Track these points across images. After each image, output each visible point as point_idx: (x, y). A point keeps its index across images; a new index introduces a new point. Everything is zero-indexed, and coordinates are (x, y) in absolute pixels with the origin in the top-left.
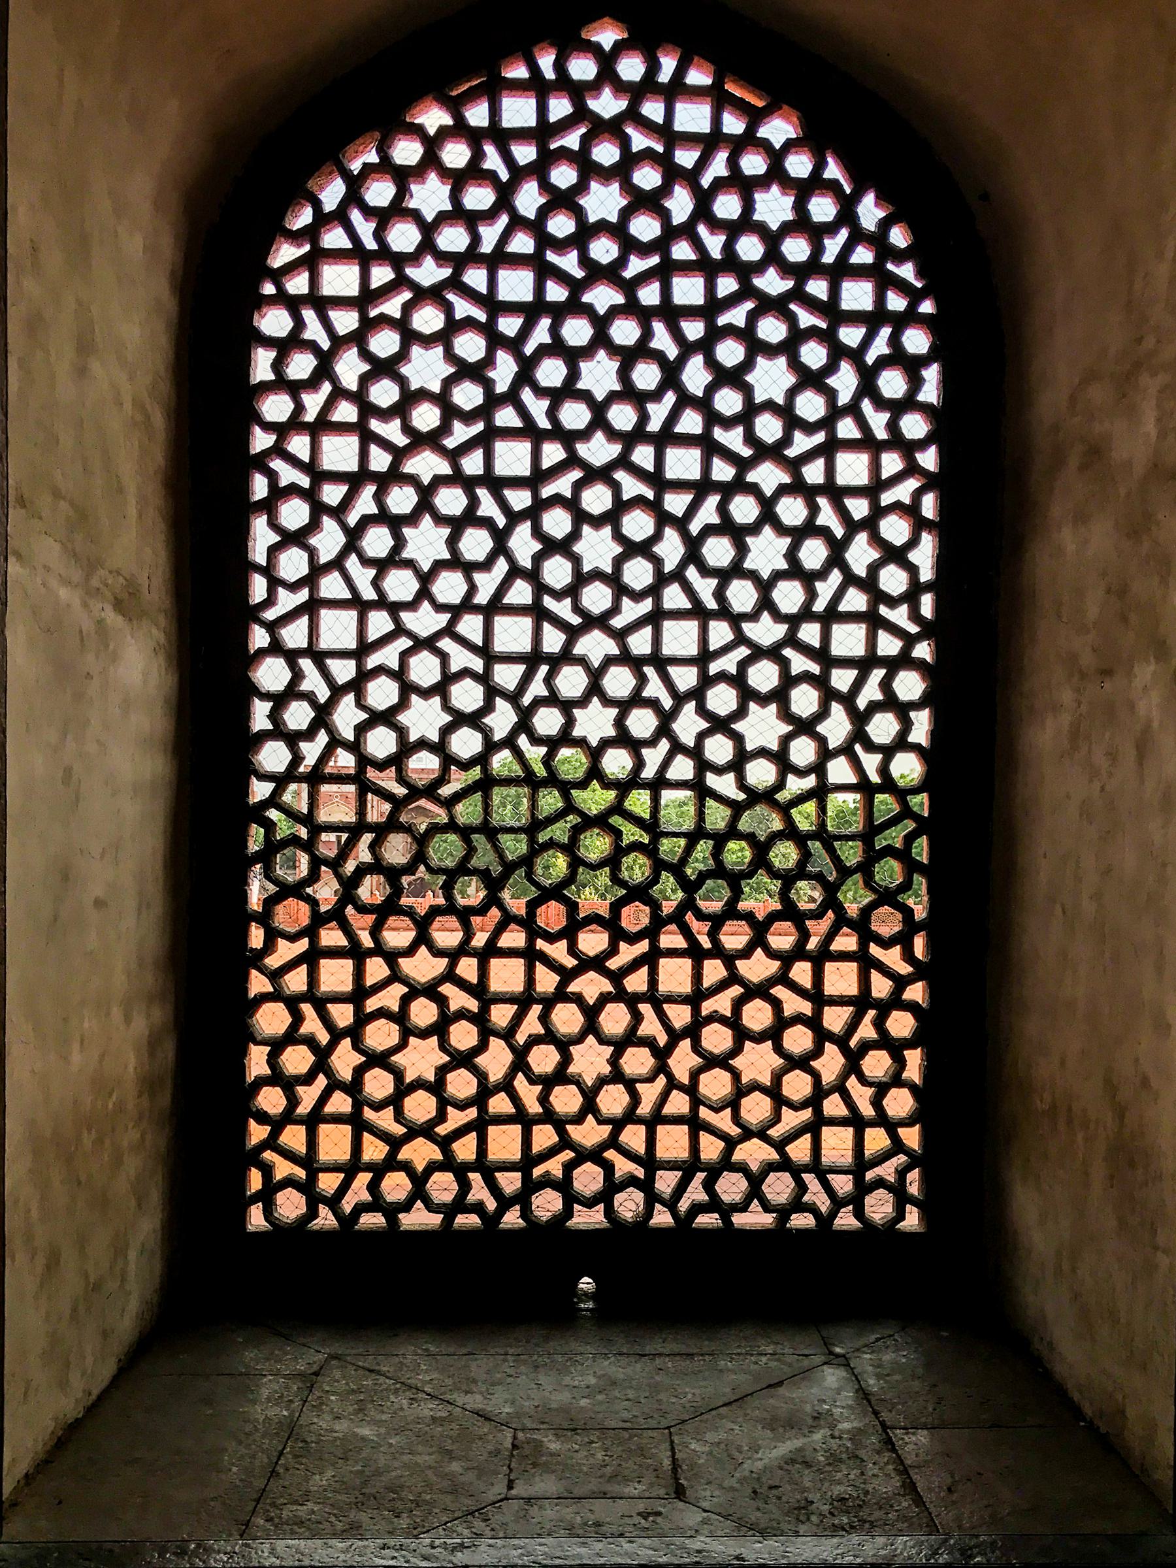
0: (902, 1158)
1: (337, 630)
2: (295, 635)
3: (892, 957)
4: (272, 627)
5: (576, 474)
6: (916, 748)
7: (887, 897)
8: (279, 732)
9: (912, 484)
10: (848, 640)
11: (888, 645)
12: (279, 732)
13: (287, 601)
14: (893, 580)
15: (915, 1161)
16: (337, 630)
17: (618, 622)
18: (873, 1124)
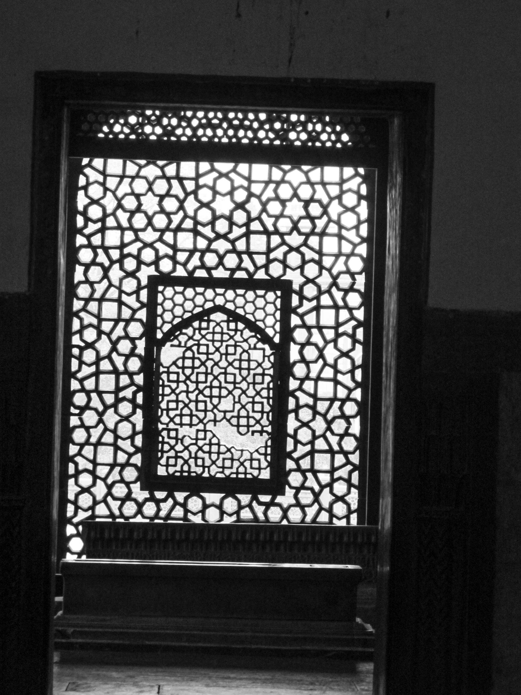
0: (349, 467)
1: (113, 238)
2: (96, 240)
3: (346, 379)
4: (89, 237)
5: (215, 175)
6: (358, 291)
7: (345, 354)
8: (87, 281)
9: (359, 180)
10: (330, 245)
11: (347, 248)
12: (87, 281)
13: (92, 227)
14: (349, 220)
15: (355, 468)
16: (113, 238)
17: (231, 236)
18: (338, 452)
